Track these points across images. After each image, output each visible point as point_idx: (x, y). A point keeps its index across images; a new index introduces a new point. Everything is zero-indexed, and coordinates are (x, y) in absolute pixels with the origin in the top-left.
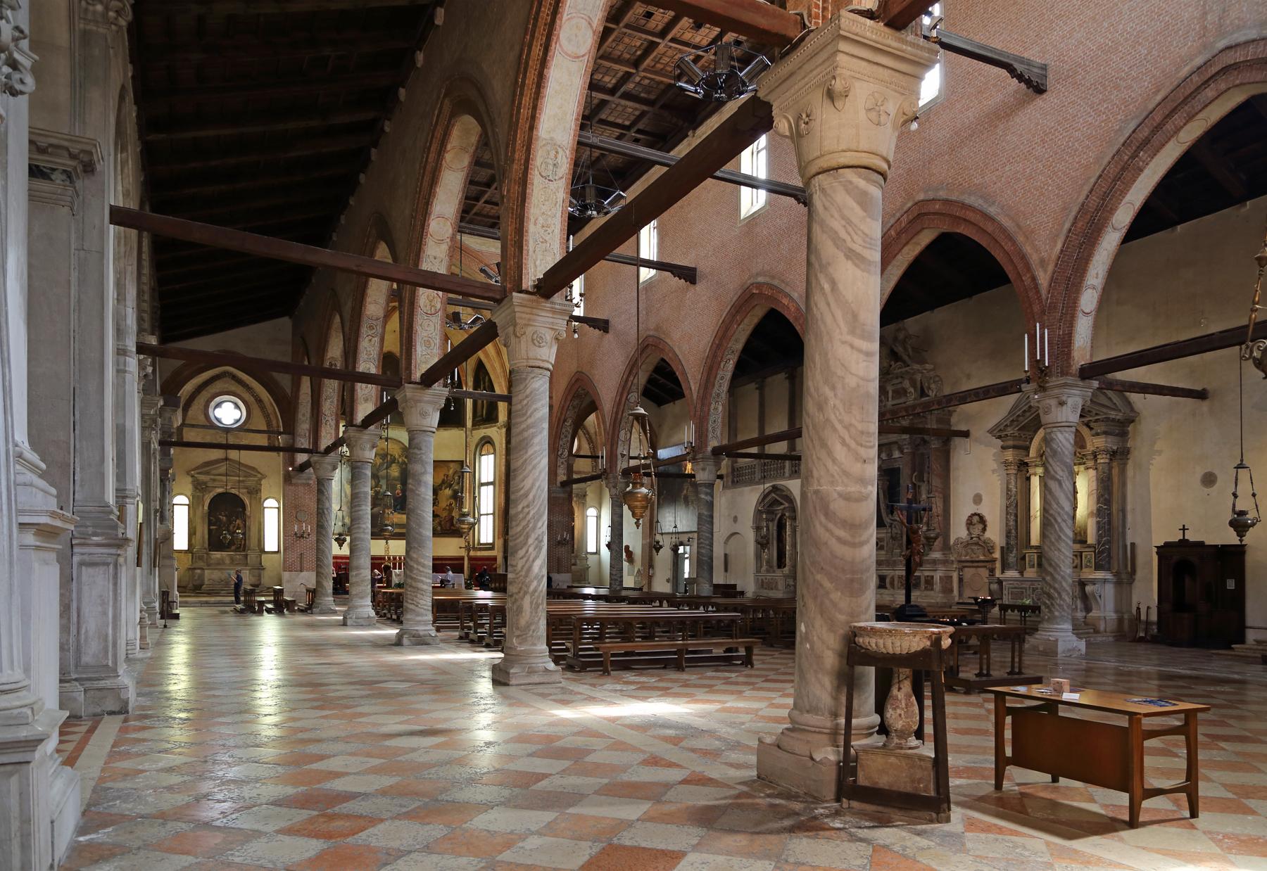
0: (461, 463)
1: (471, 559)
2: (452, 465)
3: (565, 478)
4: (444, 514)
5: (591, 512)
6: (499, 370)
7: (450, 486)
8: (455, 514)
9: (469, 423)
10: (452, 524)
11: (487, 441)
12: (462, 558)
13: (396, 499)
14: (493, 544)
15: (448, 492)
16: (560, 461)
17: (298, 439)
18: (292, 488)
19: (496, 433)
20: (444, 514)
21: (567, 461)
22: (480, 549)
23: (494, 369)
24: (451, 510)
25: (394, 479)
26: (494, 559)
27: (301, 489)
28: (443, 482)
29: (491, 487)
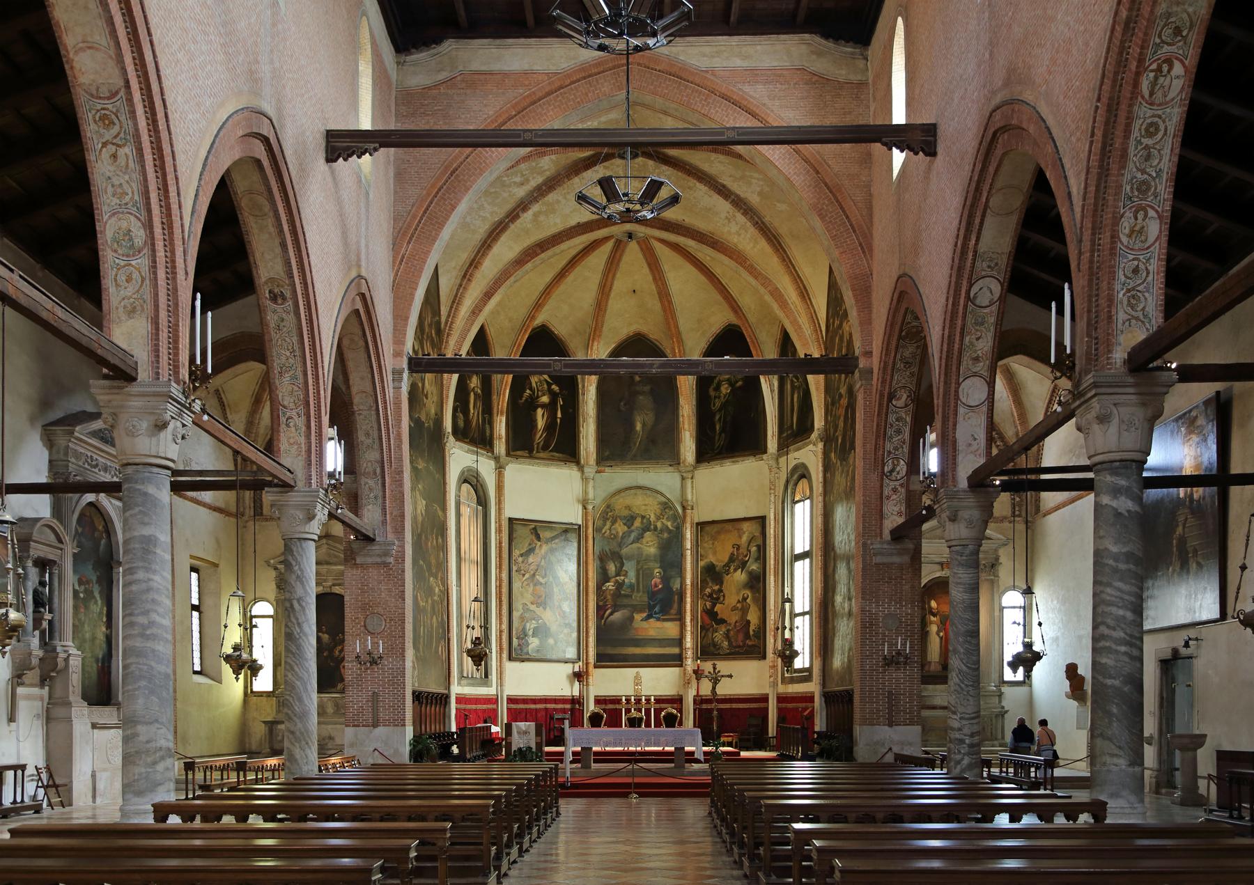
0: (762, 520)
1: (781, 699)
2: (745, 526)
3: (901, 520)
4: (733, 618)
5: (1013, 598)
6: (807, 329)
7: (743, 565)
8: (753, 617)
9: (772, 444)
10: (747, 636)
11: (801, 473)
12: (764, 699)
13: (652, 595)
14: (809, 670)
15: (740, 576)
16: (889, 485)
17: (363, 480)
18: (357, 572)
19: (810, 455)
20: (733, 618)
21: (906, 485)
22: (792, 681)
23: (799, 328)
24: (745, 611)
25: (647, 559)
26: (809, 698)
27: (373, 573)
28: (732, 559)
29: (807, 561)
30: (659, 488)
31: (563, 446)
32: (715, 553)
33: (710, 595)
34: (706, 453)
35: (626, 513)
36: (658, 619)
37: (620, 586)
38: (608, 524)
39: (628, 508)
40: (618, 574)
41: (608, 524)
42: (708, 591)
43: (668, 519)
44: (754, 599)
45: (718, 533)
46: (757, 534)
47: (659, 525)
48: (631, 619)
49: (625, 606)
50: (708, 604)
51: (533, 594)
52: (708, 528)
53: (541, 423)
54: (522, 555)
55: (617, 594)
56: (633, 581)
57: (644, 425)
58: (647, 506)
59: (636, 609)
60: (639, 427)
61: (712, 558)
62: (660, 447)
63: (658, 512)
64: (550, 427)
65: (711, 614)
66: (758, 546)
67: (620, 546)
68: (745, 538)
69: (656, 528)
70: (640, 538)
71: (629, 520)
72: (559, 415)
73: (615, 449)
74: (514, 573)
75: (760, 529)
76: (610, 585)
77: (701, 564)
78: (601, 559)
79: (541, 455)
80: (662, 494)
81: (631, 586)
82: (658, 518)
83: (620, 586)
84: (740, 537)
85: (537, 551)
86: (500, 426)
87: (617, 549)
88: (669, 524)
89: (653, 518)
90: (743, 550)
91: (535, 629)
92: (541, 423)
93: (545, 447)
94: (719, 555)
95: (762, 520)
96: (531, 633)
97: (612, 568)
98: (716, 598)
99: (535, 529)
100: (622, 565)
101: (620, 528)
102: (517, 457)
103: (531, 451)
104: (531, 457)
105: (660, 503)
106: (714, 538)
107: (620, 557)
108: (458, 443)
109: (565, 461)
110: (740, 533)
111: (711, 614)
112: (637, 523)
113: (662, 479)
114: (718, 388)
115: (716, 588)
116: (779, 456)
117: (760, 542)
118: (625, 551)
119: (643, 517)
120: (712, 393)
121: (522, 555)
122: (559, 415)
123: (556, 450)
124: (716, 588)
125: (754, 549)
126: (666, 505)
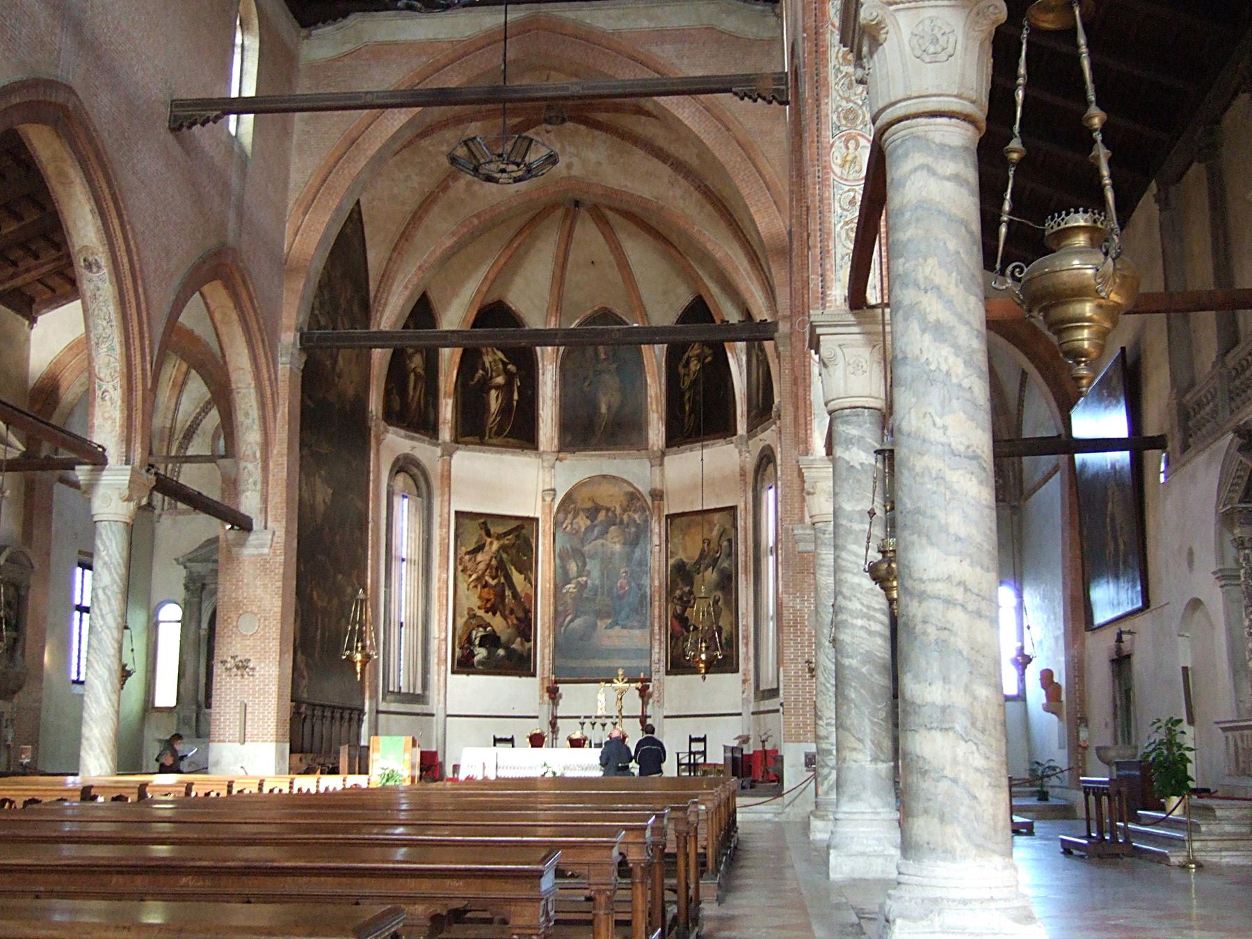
30: (625, 477)
31: (520, 432)
32: (685, 550)
33: (681, 598)
34: (678, 436)
36: (624, 627)
37: (582, 587)
38: (570, 516)
39: (592, 499)
40: (580, 575)
41: (570, 516)
42: (678, 592)
44: (727, 603)
45: (689, 526)
47: (625, 517)
48: (595, 626)
49: (586, 613)
50: (679, 609)
51: (480, 597)
52: (677, 521)
53: (494, 405)
54: (468, 553)
55: (579, 598)
56: (597, 582)
58: (610, 496)
59: (600, 614)
61: (681, 556)
63: (625, 503)
64: (505, 409)
65: (682, 620)
67: (582, 542)
69: (622, 522)
70: (604, 533)
72: (516, 397)
73: (581, 432)
74: (460, 574)
76: (570, 587)
77: (671, 562)
78: (561, 558)
79: (494, 441)
80: (630, 484)
81: (595, 590)
82: (624, 511)
83: (582, 587)
85: (487, 548)
86: (447, 409)
87: (579, 546)
89: (618, 511)
90: (714, 545)
91: (482, 637)
92: (494, 405)
93: (498, 433)
94: (689, 551)
96: (477, 642)
97: (573, 567)
98: (686, 601)
99: (484, 523)
100: (585, 564)
101: (583, 522)
102: (466, 444)
103: (482, 437)
104: (482, 443)
105: (627, 493)
107: (583, 555)
108: (391, 429)
109: (522, 448)
111: (682, 620)
112: (602, 516)
113: (632, 469)
114: (687, 365)
115: (687, 589)
118: (586, 548)
120: (682, 371)
121: (468, 553)
122: (516, 397)
123: (510, 435)
124: (687, 589)
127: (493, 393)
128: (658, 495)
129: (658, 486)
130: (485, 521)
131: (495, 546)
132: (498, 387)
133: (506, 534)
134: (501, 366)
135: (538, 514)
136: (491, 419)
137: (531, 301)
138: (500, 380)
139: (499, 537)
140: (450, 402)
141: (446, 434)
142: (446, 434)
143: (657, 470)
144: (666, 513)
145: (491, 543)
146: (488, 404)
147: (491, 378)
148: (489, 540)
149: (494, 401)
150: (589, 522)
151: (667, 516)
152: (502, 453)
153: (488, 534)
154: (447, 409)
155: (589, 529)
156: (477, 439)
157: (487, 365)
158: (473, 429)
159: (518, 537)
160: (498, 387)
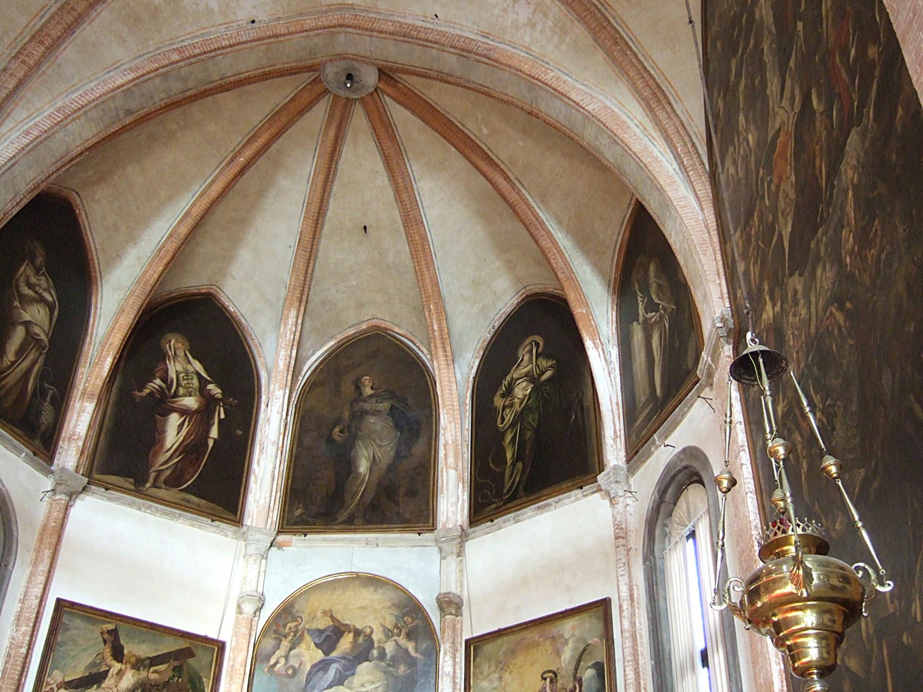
0: (603, 607)
2: (568, 627)
35: (323, 623)
38: (285, 644)
41: (285, 644)
43: (409, 636)
45: (512, 652)
46: (594, 640)
47: (389, 648)
52: (489, 648)
57: (374, 462)
58: (369, 614)
60: (363, 467)
62: (400, 503)
63: (390, 622)
66: (599, 667)
68: (568, 654)
69: (382, 656)
71: (329, 639)
75: (599, 627)
82: (389, 634)
84: (558, 653)
85: (109, 682)
86: (81, 418)
88: (410, 646)
95: (603, 607)
99: (114, 633)
106: (502, 666)
110: (557, 643)
112: (346, 643)
116: (631, 470)
117: (601, 656)
119: (357, 633)
125: (588, 674)
126: (410, 608)
127: (174, 419)
128: (450, 604)
129: (454, 589)
130: (116, 630)
131: (129, 678)
132: (184, 412)
133: (154, 661)
134: (195, 382)
135: (225, 636)
136: (162, 458)
137: (256, 288)
138: (191, 402)
139: (139, 664)
140: (90, 407)
141: (69, 455)
142: (69, 455)
143: (452, 563)
144: (467, 636)
145: (120, 673)
146: (163, 432)
147: (176, 395)
148: (118, 666)
149: (174, 432)
150: (319, 655)
151: (468, 643)
152: (173, 517)
153: (118, 655)
154: (81, 418)
155: (322, 666)
156: (128, 483)
157: (172, 374)
158: (123, 460)
159: (178, 670)
160: (184, 412)
